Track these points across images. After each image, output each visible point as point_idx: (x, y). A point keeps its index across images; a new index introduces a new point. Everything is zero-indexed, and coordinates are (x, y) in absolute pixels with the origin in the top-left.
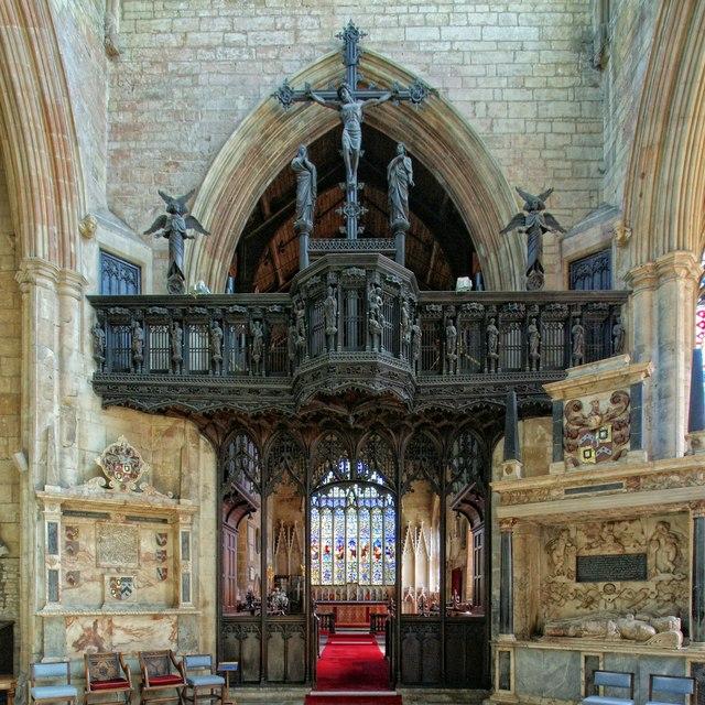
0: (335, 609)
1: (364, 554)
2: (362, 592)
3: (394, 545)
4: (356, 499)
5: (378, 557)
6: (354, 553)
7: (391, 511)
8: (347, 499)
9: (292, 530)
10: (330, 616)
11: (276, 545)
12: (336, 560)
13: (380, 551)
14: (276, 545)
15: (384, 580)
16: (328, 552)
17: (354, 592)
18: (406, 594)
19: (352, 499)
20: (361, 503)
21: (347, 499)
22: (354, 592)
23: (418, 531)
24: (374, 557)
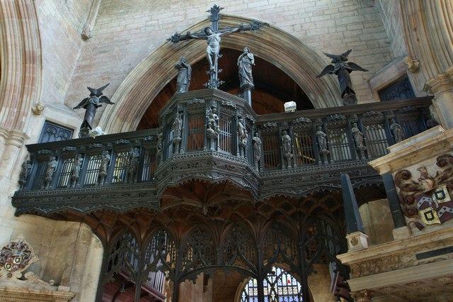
4: (277, 296)
19: (273, 296)
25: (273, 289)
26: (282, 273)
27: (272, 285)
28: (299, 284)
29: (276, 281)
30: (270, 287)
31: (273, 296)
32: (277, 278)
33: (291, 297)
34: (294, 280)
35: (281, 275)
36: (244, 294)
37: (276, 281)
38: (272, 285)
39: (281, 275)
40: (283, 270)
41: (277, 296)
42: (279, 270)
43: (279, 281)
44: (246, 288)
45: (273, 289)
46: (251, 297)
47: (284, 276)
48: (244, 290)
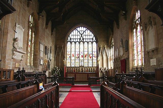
0: (75, 75)
1: (86, 57)
2: (85, 69)
3: (96, 54)
4: (83, 39)
5: (90, 57)
6: (82, 56)
7: (94, 43)
8: (80, 39)
9: (61, 49)
10: (73, 78)
11: (55, 54)
12: (76, 59)
13: (91, 55)
14: (55, 54)
15: (93, 65)
16: (73, 56)
17: (82, 69)
18: (100, 69)
19: (82, 39)
20: (85, 40)
21: (80, 39)
22: (82, 69)
23: (104, 49)
24: (89, 58)
25: (82, 36)
26: (86, 30)
27: (81, 35)
28: (93, 34)
29: (83, 33)
30: (80, 35)
31: (82, 39)
32: (84, 32)
33: (89, 40)
34: (91, 33)
35: (85, 31)
36: (69, 37)
37: (83, 33)
38: (81, 35)
39: (85, 31)
40: (86, 29)
41: (83, 39)
42: (85, 28)
43: (85, 33)
44: (70, 35)
45: (82, 36)
46: (72, 39)
47: (87, 31)
48: (69, 36)
